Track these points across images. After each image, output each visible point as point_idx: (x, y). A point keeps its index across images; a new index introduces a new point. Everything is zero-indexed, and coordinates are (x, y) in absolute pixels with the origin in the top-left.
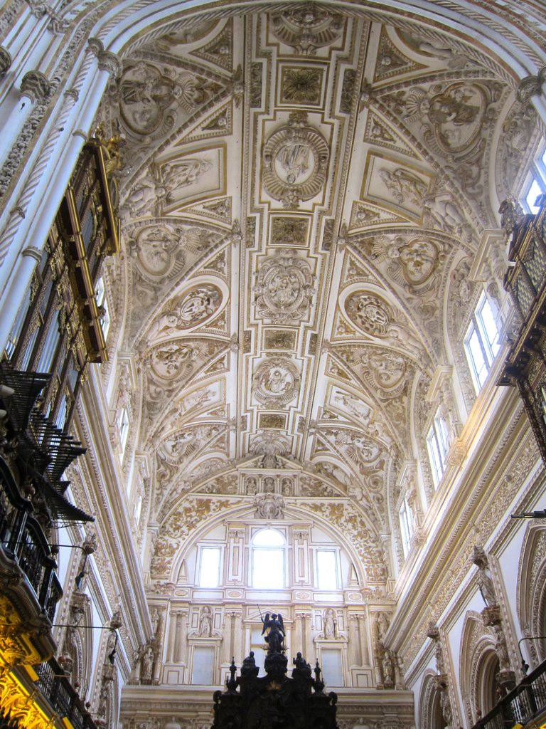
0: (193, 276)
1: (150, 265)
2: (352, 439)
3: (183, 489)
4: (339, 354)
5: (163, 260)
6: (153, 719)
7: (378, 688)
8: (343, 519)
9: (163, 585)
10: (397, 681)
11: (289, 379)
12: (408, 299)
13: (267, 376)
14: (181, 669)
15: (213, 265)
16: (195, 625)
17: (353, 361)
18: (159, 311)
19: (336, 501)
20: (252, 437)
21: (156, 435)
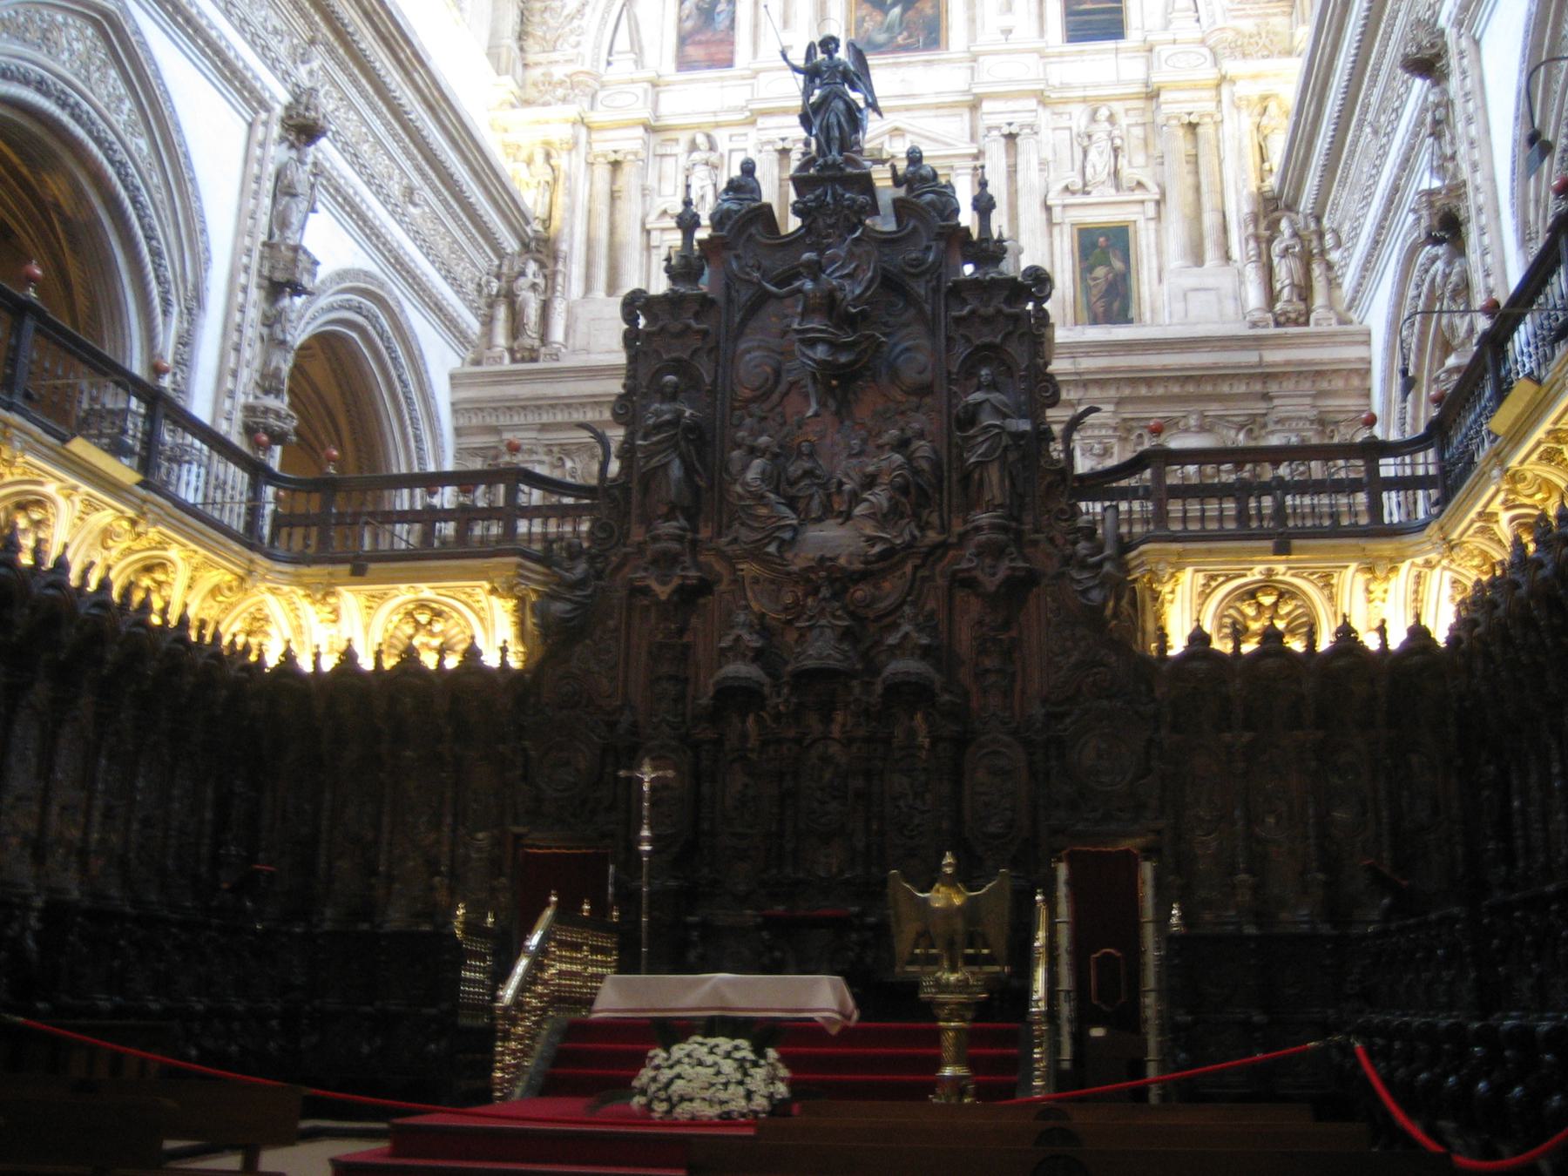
7: (1254, 325)
9: (562, 83)
10: (1319, 300)
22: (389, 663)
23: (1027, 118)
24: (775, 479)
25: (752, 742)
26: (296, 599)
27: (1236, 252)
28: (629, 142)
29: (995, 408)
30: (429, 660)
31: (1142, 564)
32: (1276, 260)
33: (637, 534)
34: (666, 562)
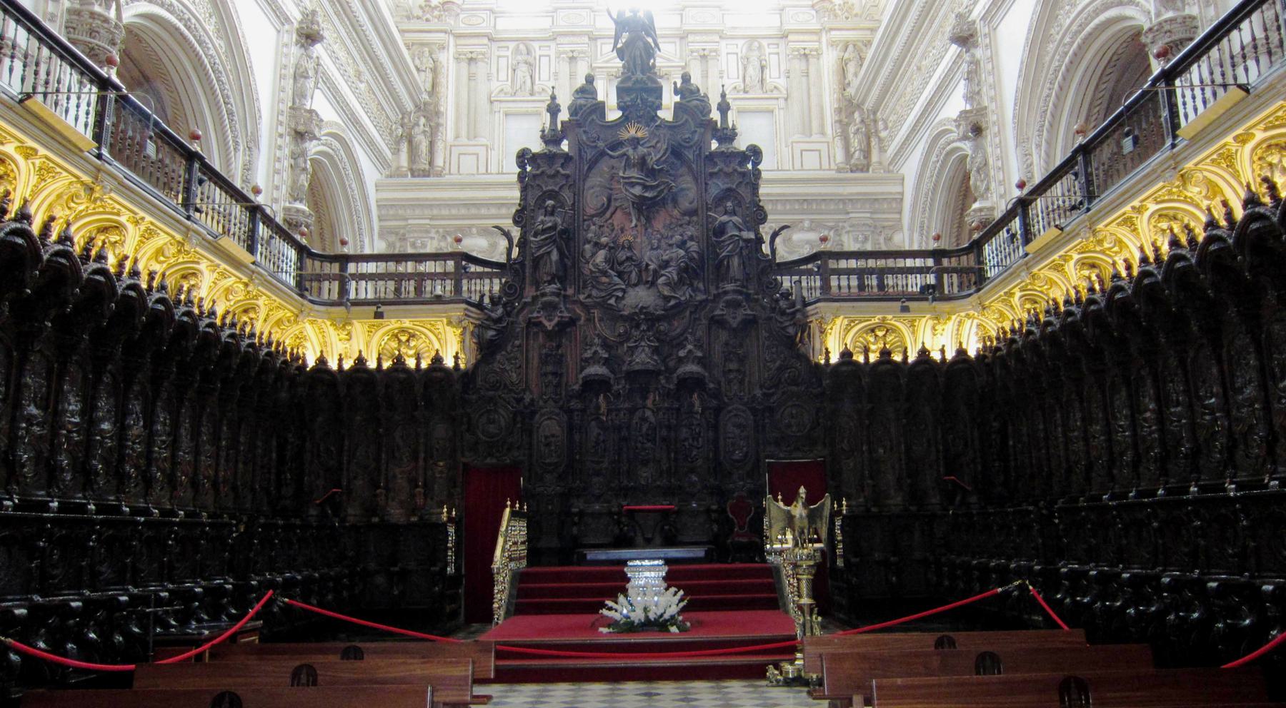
6: (438, 232)
7: (839, 170)
9: (436, 7)
10: (875, 157)
14: (482, 152)
16: (503, 76)
22: (386, 365)
23: (713, 46)
24: (611, 261)
25: (603, 408)
26: (324, 326)
27: (829, 131)
28: (478, 46)
29: (734, 224)
30: (411, 363)
31: (817, 313)
32: (852, 135)
33: (530, 292)
34: (550, 308)
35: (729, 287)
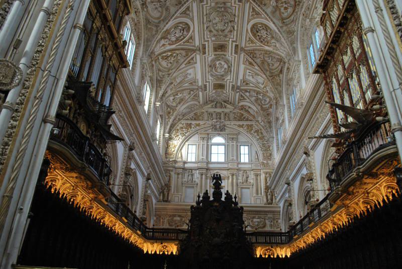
0: (175, 19)
1: (152, 14)
2: (257, 94)
3: (179, 119)
4: (249, 54)
5: (159, 12)
7: (265, 204)
8: (253, 131)
10: (274, 201)
11: (226, 66)
12: (281, 27)
13: (215, 65)
15: (184, 13)
17: (255, 57)
18: (159, 37)
19: (249, 123)
20: (210, 94)
21: (163, 95)
22: (161, 253)
27: (263, 193)
28: (181, 171)
30: (166, 253)
33: (192, 238)
35: (235, 239)
